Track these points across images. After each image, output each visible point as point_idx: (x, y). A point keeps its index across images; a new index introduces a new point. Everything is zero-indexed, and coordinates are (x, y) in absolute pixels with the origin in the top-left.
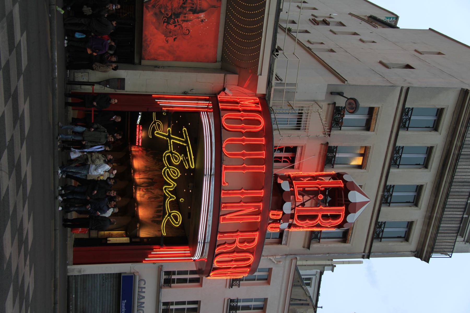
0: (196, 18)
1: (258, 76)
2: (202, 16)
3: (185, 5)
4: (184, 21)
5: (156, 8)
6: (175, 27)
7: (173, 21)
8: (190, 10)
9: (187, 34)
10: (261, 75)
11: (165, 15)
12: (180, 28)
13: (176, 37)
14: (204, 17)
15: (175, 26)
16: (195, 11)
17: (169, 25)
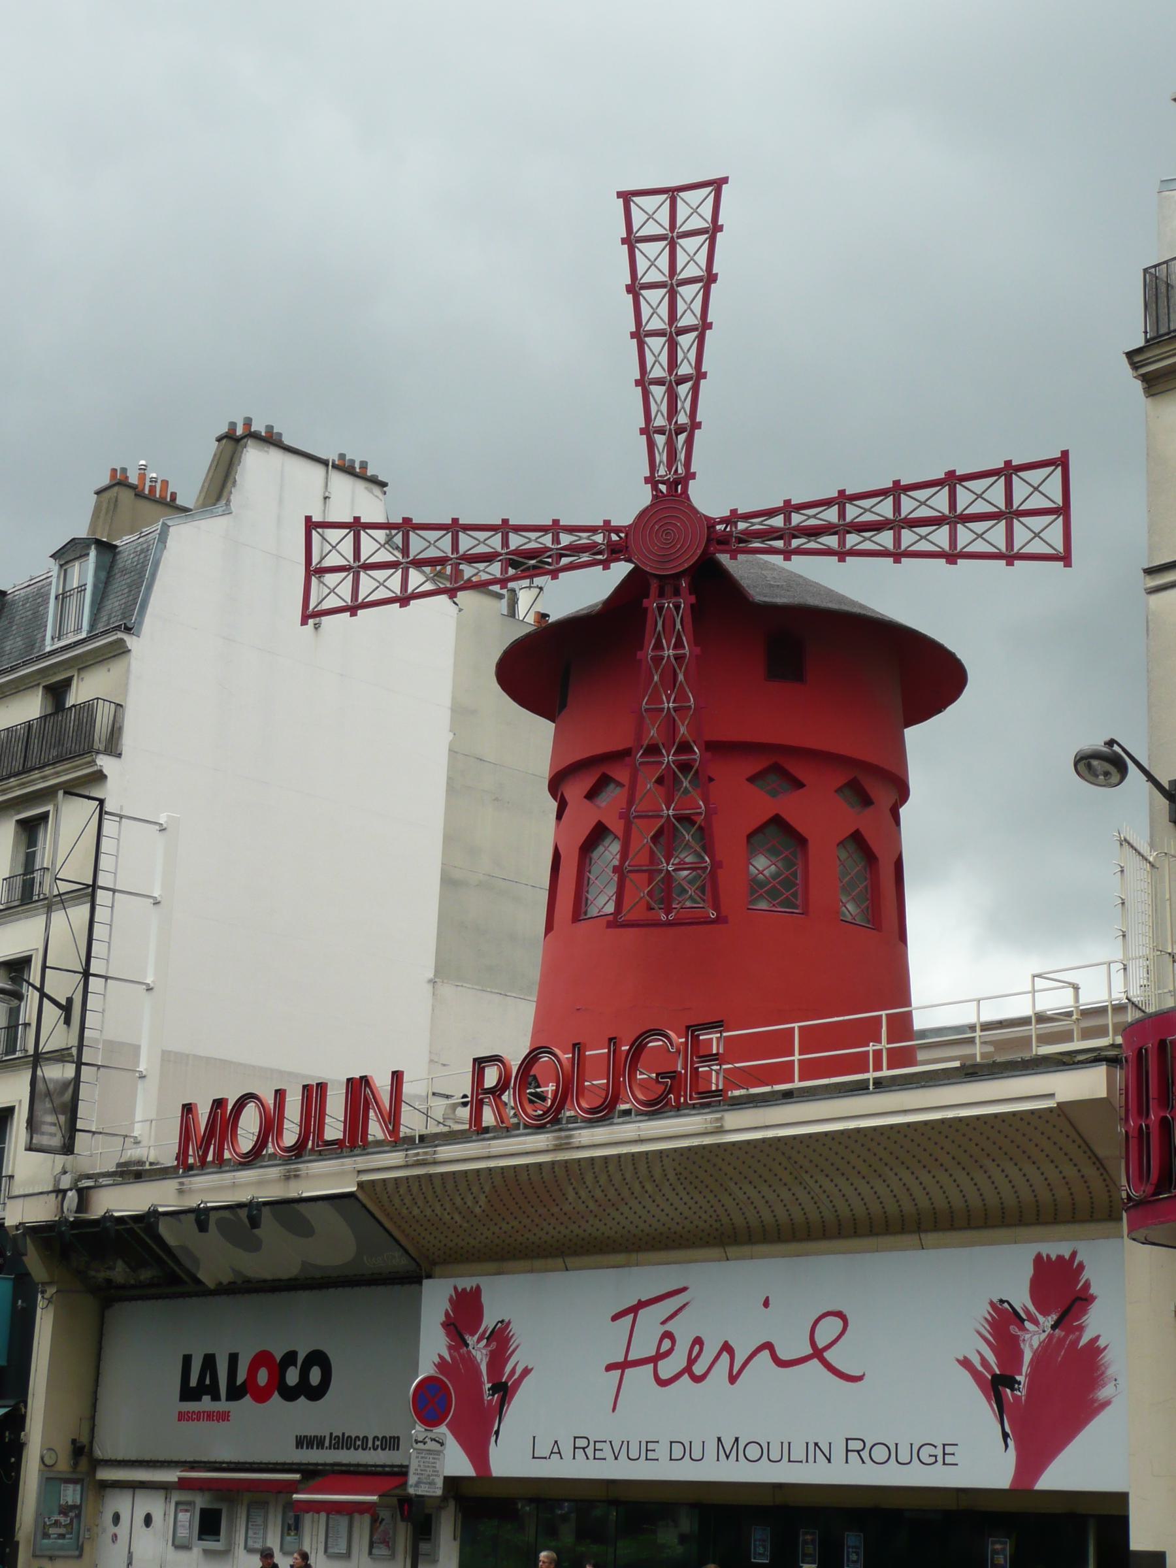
1: (1058, 1104)
10: (1052, 1095)
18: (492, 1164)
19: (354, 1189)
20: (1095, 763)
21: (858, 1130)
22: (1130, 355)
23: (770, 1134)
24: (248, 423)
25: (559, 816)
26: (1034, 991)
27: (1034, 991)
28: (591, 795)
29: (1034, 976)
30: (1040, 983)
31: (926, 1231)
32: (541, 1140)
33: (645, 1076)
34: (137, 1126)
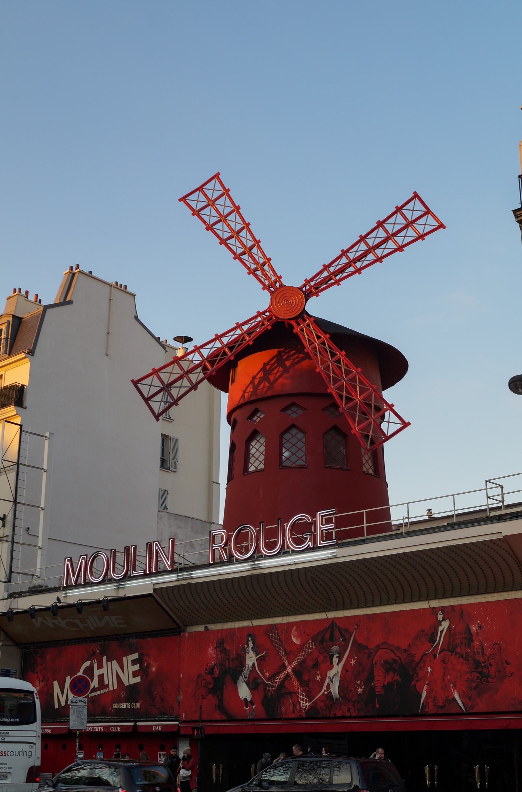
0: (478, 637)
1: (503, 536)
2: (474, 628)
3: (464, 654)
4: (483, 653)
5: (472, 695)
6: (492, 666)
7: (485, 669)
8: (469, 647)
9: (499, 646)
10: (502, 532)
11: (479, 681)
12: (493, 657)
13: (505, 663)
14: (475, 626)
15: (491, 665)
16: (469, 639)
17: (490, 674)
18: (221, 577)
19: (152, 592)
20: (518, 383)
21: (404, 554)
22: (515, 211)
23: (360, 557)
24: (78, 267)
25: (233, 429)
26: (487, 489)
27: (487, 489)
28: (251, 417)
29: (487, 481)
30: (489, 485)
31: (430, 600)
32: (246, 566)
33: (296, 536)
34: (38, 570)
